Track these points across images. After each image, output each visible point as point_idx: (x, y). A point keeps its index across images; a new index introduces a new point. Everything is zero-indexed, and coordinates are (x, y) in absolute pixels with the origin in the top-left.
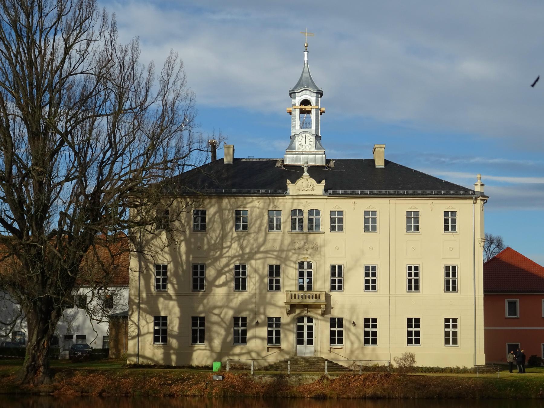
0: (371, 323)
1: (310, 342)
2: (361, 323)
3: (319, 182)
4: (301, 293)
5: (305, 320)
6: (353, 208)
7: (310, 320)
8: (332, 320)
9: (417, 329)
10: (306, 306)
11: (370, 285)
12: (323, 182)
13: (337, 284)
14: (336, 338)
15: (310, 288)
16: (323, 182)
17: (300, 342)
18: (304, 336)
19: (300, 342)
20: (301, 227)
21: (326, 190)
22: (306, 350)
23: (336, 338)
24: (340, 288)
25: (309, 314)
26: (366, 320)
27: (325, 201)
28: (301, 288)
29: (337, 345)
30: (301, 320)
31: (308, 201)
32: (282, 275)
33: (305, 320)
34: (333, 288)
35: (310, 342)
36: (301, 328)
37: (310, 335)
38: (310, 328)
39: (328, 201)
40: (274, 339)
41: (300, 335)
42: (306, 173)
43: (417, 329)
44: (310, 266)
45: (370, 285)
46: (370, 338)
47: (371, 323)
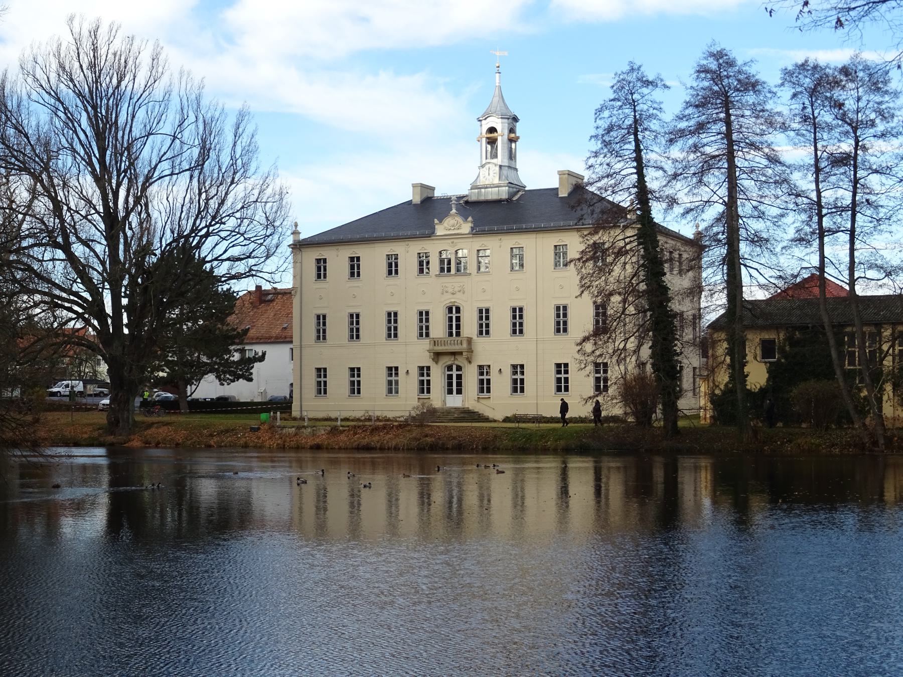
0: (518, 369)
1: (459, 392)
2: (508, 371)
3: (466, 219)
4: (451, 338)
5: (454, 367)
6: (497, 248)
7: (459, 368)
8: (481, 367)
9: (566, 376)
10: (454, 354)
11: (517, 329)
12: (470, 219)
13: (484, 329)
14: (485, 386)
15: (458, 334)
16: (470, 219)
17: (450, 392)
18: (455, 385)
19: (450, 392)
20: (449, 270)
21: (472, 228)
22: (455, 401)
23: (485, 386)
24: (487, 333)
25: (456, 362)
26: (514, 367)
27: (471, 240)
28: (451, 334)
29: (485, 394)
30: (450, 368)
31: (455, 241)
32: (430, 320)
33: (454, 367)
34: (481, 333)
35: (459, 392)
36: (450, 377)
37: (459, 384)
38: (459, 377)
39: (474, 239)
40: (425, 387)
41: (450, 384)
42: (454, 211)
43: (566, 376)
44: (458, 310)
45: (517, 329)
46: (518, 386)
47: (518, 369)
